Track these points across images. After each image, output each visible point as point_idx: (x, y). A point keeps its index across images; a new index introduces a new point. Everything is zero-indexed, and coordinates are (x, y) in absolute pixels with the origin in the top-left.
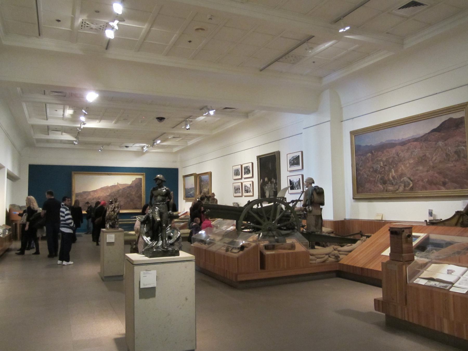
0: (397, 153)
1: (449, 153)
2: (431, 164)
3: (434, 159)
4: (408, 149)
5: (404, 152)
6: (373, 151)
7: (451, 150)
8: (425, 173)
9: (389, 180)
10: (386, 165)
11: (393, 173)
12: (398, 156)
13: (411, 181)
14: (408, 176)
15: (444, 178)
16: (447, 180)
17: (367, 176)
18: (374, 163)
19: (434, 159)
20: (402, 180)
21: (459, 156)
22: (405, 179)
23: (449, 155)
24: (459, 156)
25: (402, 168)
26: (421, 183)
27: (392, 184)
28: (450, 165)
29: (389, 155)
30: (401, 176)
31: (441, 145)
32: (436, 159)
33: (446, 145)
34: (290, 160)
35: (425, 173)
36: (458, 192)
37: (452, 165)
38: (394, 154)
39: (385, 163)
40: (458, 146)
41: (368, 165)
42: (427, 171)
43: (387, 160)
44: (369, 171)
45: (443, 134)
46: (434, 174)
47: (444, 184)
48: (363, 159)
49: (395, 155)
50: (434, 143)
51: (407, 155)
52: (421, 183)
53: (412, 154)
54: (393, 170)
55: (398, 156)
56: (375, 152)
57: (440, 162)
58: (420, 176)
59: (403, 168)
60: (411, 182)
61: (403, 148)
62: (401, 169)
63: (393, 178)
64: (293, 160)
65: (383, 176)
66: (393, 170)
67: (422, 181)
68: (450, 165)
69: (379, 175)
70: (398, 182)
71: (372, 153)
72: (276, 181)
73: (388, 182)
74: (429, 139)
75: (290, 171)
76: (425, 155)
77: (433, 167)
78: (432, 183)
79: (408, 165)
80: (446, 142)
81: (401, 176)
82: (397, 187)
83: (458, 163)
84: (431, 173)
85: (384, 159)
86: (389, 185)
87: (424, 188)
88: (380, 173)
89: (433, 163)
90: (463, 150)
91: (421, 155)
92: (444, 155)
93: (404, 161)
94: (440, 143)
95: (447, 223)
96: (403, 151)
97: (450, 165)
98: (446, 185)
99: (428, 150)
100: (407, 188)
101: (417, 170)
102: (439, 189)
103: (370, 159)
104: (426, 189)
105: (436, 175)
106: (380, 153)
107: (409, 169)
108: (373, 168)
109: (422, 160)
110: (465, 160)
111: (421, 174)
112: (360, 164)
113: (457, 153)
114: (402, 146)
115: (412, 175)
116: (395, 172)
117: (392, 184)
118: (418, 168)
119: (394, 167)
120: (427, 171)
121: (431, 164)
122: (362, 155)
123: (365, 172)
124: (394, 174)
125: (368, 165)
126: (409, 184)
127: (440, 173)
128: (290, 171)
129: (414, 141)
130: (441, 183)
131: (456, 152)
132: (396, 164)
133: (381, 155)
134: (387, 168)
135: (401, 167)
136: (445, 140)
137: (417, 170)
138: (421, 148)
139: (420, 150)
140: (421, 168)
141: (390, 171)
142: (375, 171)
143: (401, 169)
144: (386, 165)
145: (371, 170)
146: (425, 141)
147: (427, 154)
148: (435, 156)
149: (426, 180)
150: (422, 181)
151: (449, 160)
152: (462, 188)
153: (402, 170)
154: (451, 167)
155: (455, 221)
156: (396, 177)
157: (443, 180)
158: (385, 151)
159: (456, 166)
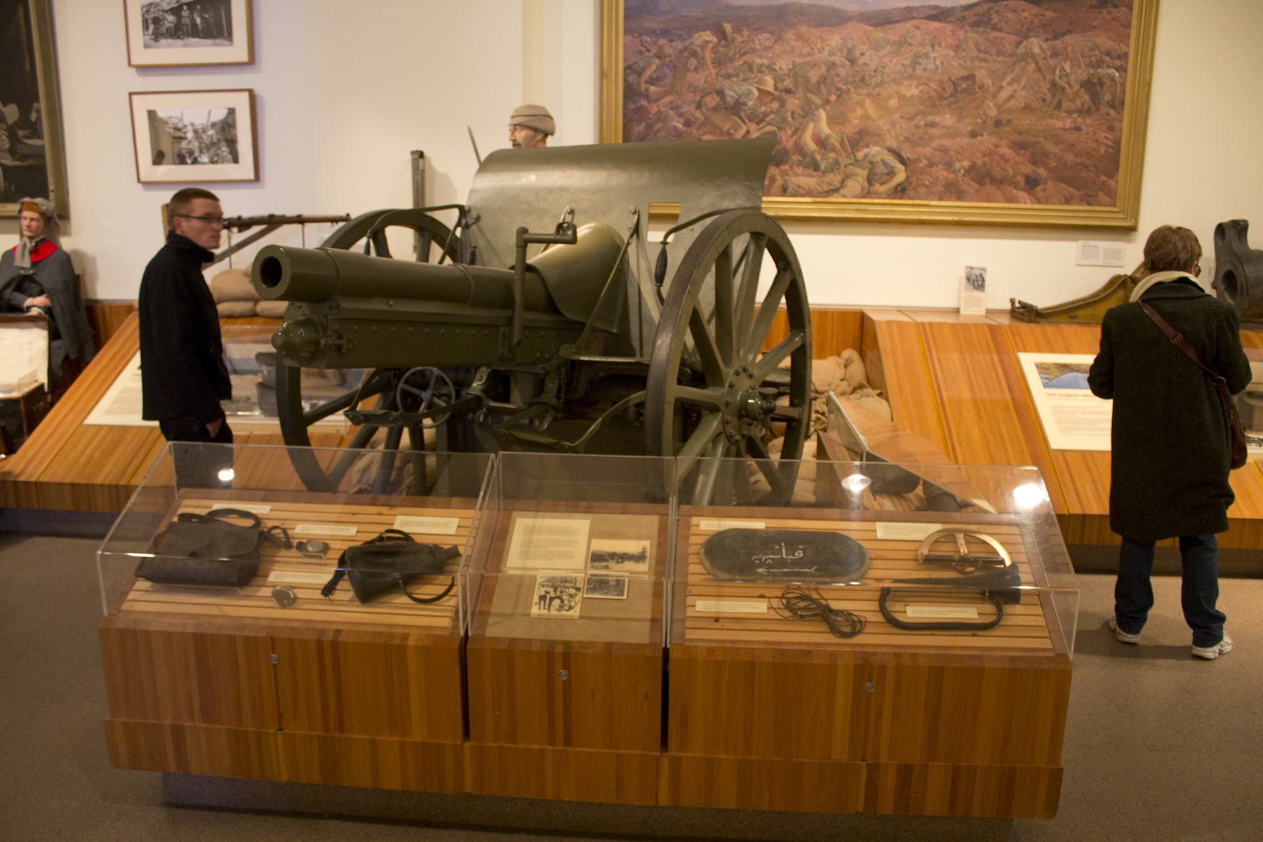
0: (850, 51)
1: (1062, 83)
2: (993, 112)
3: (1004, 94)
4: (902, 42)
5: (882, 53)
6: (728, 27)
7: (1073, 72)
8: (964, 141)
9: (800, 149)
10: (789, 91)
11: (822, 124)
12: (853, 62)
13: (902, 161)
14: (893, 143)
15: (1034, 164)
16: (1042, 172)
17: (687, 124)
18: (728, 76)
19: (1004, 94)
20: (860, 155)
21: (1095, 98)
22: (875, 151)
23: (1063, 89)
24: (1095, 98)
25: (863, 110)
26: (942, 173)
27: (816, 167)
28: (1061, 122)
29: (809, 54)
30: (858, 140)
31: (1036, 50)
32: (1011, 97)
33: (1055, 54)
34: (147, 9)
35: (964, 141)
36: (1078, 213)
37: (1068, 124)
38: (832, 53)
39: (788, 83)
40: (1099, 64)
41: (699, 79)
42: (973, 135)
43: (794, 73)
44: (699, 106)
45: (1049, 14)
46: (997, 146)
47: (1031, 184)
48: (668, 50)
49: (837, 59)
50: (1013, 38)
51: (895, 64)
52: (942, 173)
53: (915, 63)
54: (822, 114)
55: (853, 62)
56: (737, 30)
57: (1027, 108)
58: (944, 150)
59: (871, 111)
60: (901, 167)
61: (878, 34)
62: (859, 112)
63: (822, 143)
64: (176, 11)
65: (773, 133)
66: (822, 114)
67: (949, 165)
68: (1060, 124)
69: (753, 126)
70: (844, 160)
71: (721, 34)
72: (25, 109)
73: (796, 157)
74: (995, 20)
75: (144, 69)
76: (971, 77)
77: (998, 123)
78: (985, 179)
79: (893, 103)
80: (1058, 44)
81: (858, 140)
82: (835, 179)
83: (1088, 121)
84: (987, 140)
85: (783, 65)
86: (800, 170)
87: (953, 191)
88: (759, 119)
89: (998, 107)
90: (1113, 79)
91: (957, 73)
92: (1045, 88)
93: (880, 84)
94: (1036, 45)
95: (1081, 313)
96: (876, 47)
97: (1061, 122)
98: (1038, 189)
99: (985, 60)
100: (878, 188)
101: (933, 125)
102: (1011, 200)
103: (708, 55)
104: (960, 196)
105: (1006, 150)
106: (764, 38)
107: (896, 116)
108: (721, 93)
109: (960, 91)
110: (1112, 112)
111: (947, 143)
112: (648, 73)
113: (1091, 86)
114: (876, 25)
115: (906, 139)
116: (831, 121)
117: (816, 167)
118: (937, 119)
119: (828, 102)
120: (973, 135)
121: (993, 112)
122: (665, 33)
123: (675, 108)
124: (825, 129)
125: (699, 79)
126: (891, 173)
127: (1019, 146)
128: (144, 69)
129: (932, 18)
130: (1021, 180)
131: (1088, 85)
132: (841, 94)
133: (766, 48)
134: (793, 103)
135: (861, 104)
136: (1055, 38)
137: (933, 125)
138: (957, 48)
139: (952, 53)
140: (948, 119)
141: (808, 112)
142: (736, 108)
143: (859, 112)
144: (789, 91)
145: (711, 101)
146: (976, 24)
147: (981, 75)
148: (1009, 84)
149: (966, 164)
150: (949, 165)
151: (1059, 106)
152: (1089, 204)
153: (866, 116)
154: (1064, 130)
156: (835, 140)
157: (1028, 169)
158: (790, 35)
159: (1078, 129)
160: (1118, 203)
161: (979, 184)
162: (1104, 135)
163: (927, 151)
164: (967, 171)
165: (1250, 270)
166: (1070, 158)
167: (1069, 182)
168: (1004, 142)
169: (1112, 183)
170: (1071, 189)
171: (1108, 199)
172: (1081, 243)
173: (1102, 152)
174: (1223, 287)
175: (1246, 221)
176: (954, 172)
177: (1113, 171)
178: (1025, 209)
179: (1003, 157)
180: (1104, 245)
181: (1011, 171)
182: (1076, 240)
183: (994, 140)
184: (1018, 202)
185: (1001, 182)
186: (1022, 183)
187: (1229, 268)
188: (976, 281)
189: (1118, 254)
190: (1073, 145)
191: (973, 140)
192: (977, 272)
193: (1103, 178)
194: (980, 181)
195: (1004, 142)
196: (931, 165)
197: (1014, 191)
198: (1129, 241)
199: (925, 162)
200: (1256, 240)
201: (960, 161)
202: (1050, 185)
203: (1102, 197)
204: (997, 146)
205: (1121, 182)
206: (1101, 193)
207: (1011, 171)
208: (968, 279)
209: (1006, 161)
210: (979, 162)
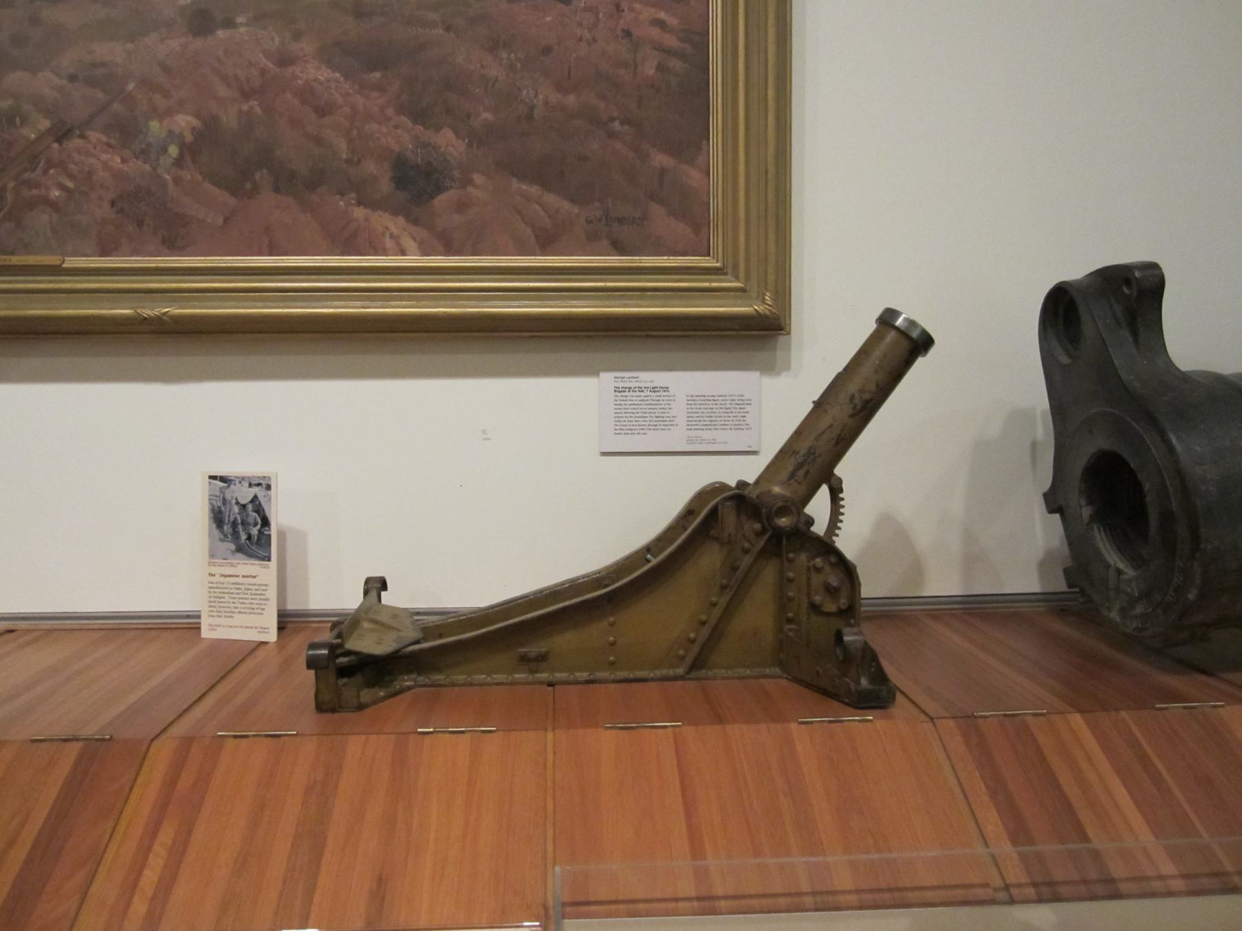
15: (420, 116)
36: (581, 281)
46: (285, 60)
47: (416, 187)
52: (100, 157)
67: (126, 132)
87: (152, 219)
95: (565, 641)
98: (440, 201)
105: (315, 73)
111: (111, 51)
149: (184, 122)
150: (126, 132)
152: (620, 248)
155: (671, 616)
157: (400, 135)
160: (716, 241)
161: (234, 191)
162: (647, 13)
163: (46, 83)
164: (191, 151)
165: (1193, 449)
166: (541, 94)
167: (547, 174)
168: (306, 47)
169: (693, 176)
170: (551, 199)
171: (682, 229)
172: (608, 379)
173: (650, 70)
174: (1086, 512)
175: (1154, 266)
176: (143, 154)
177: (689, 140)
178: (403, 271)
179: (307, 94)
180: (686, 385)
181: (342, 145)
182: (594, 372)
183: (273, 39)
184: (375, 249)
185: (312, 186)
186: (385, 186)
187: (1100, 442)
188: (242, 523)
189: (736, 411)
190: (547, 50)
191: (198, 44)
192: (245, 494)
193: (660, 159)
194: (239, 182)
195: (306, 47)
196: (62, 133)
197: (359, 213)
198: (769, 368)
199: (45, 124)
200: (1196, 337)
201: (155, 113)
202: (481, 187)
203: (662, 222)
204: (285, 60)
205: (719, 168)
206: (657, 210)
207: (342, 145)
208: (218, 518)
209: (323, 111)
210: (229, 118)
